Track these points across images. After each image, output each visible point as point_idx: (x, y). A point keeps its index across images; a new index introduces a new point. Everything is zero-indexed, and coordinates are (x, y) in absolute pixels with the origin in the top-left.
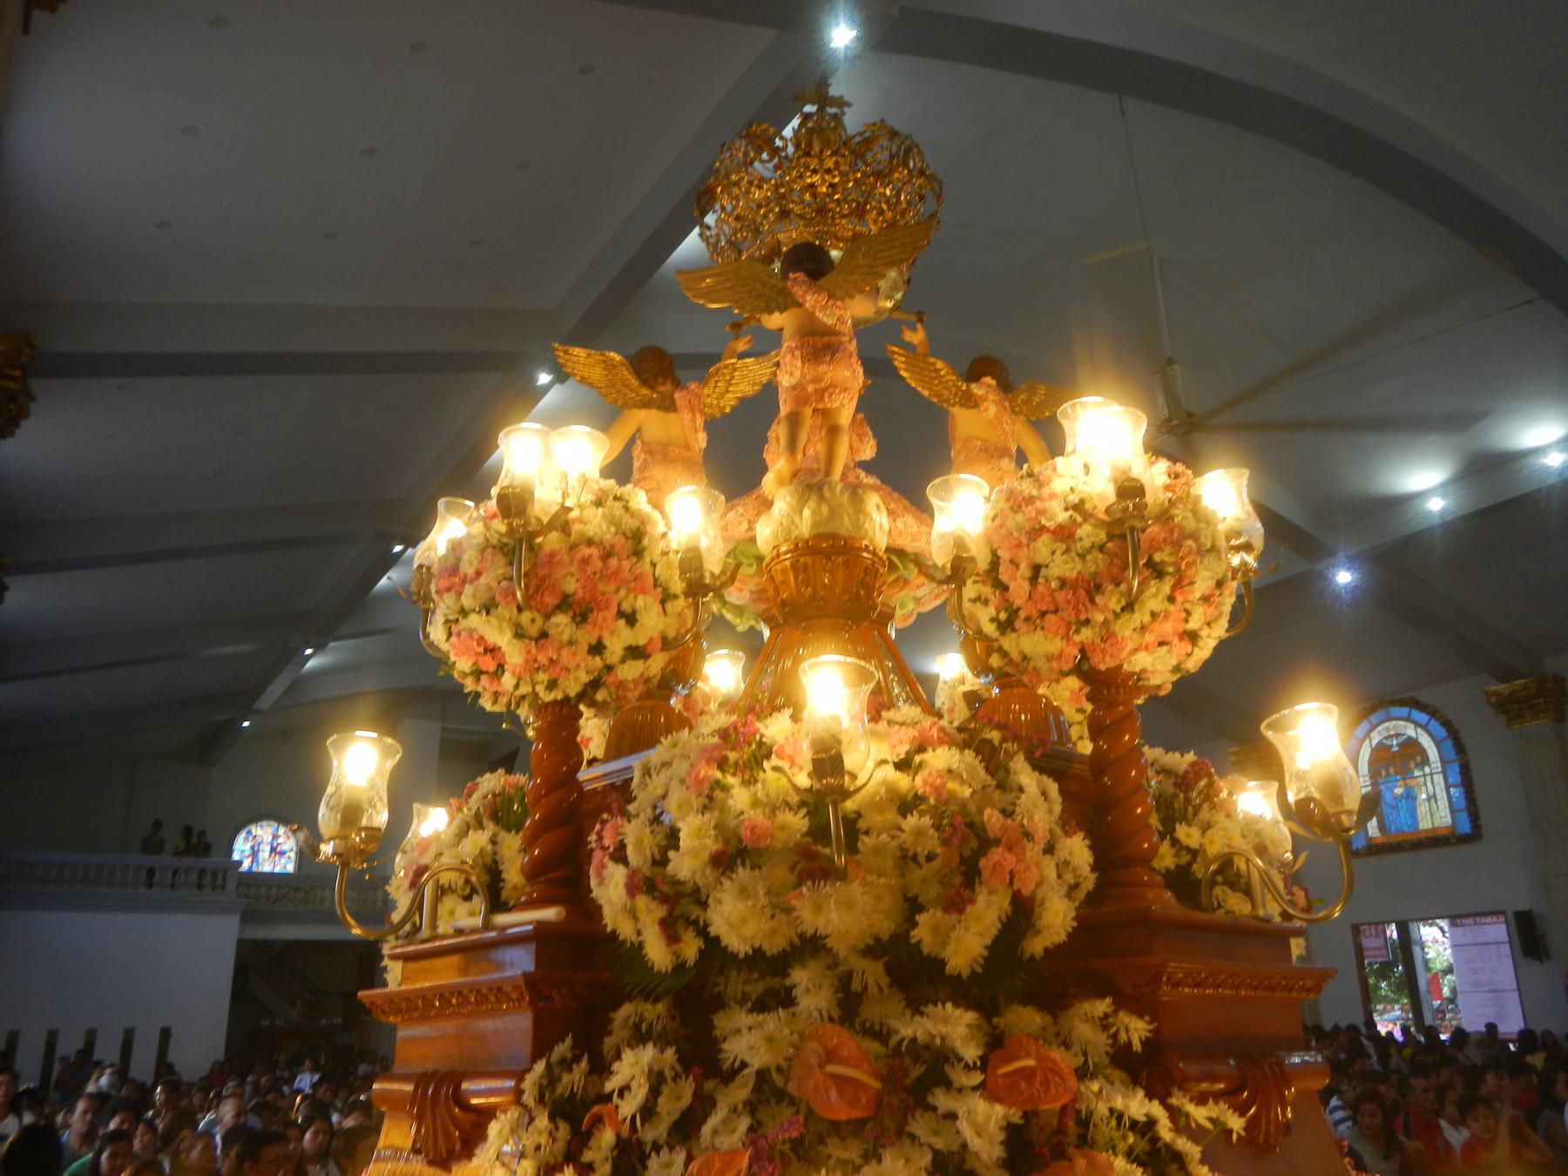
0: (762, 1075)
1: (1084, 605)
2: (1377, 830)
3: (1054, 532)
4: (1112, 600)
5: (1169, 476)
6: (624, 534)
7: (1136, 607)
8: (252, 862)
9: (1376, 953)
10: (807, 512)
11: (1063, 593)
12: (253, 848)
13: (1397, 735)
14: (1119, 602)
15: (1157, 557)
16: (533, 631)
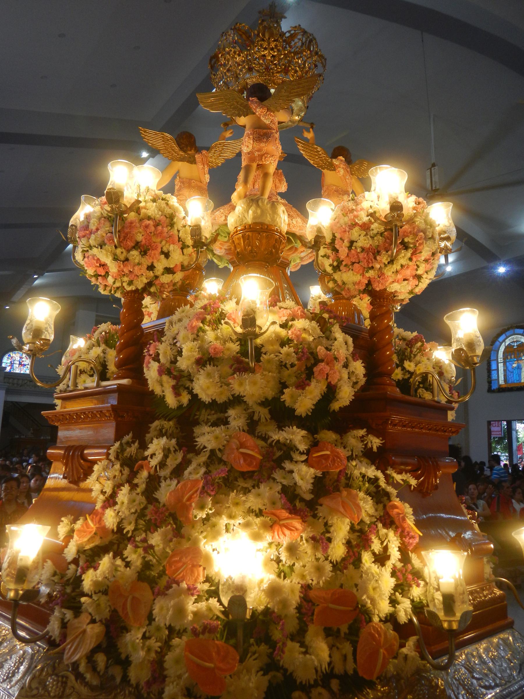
0: (212, 451)
1: (371, 260)
2: (503, 382)
3: (361, 226)
4: (384, 258)
5: (416, 203)
6: (165, 216)
7: (395, 262)
8: (11, 368)
9: (497, 433)
10: (251, 212)
11: (362, 254)
12: (11, 362)
13: (517, 341)
14: (387, 259)
15: (406, 240)
16: (122, 257)
